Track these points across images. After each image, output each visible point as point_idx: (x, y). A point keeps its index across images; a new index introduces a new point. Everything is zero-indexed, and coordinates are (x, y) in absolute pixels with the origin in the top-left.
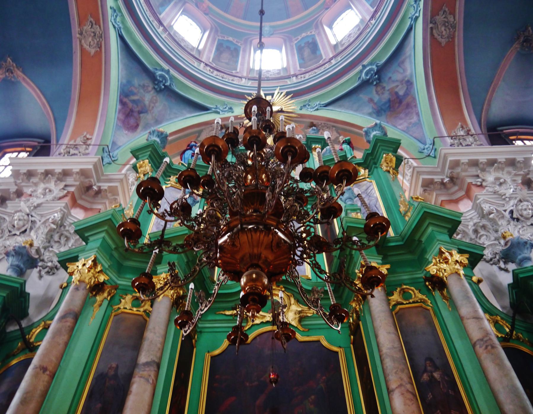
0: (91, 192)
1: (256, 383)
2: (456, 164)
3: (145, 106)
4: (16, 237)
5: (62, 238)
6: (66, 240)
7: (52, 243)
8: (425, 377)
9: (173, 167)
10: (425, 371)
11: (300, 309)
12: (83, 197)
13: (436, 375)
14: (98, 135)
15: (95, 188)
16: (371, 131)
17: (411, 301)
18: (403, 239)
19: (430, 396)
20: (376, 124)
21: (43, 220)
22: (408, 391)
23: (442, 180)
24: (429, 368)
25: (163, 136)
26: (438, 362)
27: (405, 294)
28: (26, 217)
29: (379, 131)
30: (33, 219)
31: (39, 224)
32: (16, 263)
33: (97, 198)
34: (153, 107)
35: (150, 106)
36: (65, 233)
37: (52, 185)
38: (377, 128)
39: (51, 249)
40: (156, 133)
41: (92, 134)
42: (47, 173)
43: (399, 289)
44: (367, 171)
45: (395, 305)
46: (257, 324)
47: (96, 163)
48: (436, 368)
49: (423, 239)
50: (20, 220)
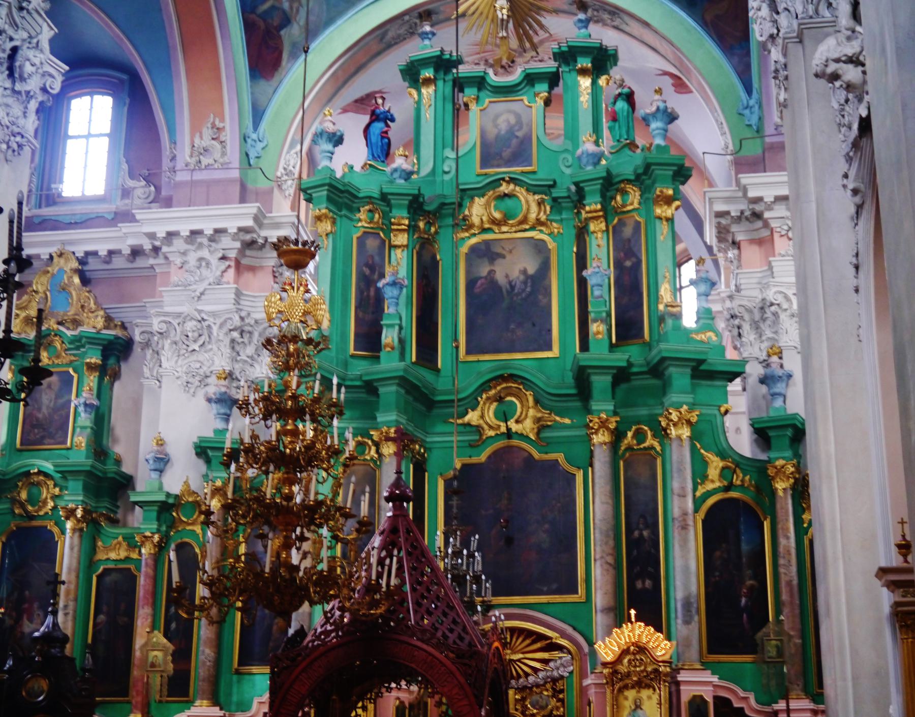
0: (255, 246)
1: (491, 511)
2: (759, 200)
3: (284, 12)
4: (195, 353)
5: (244, 335)
6: (250, 337)
7: (237, 348)
8: (636, 534)
9: (361, 195)
10: (638, 528)
11: (539, 415)
12: (248, 252)
13: (645, 533)
14: (232, 119)
15: (261, 241)
16: (651, 118)
17: (642, 446)
18: (648, 364)
19: (635, 552)
20: (658, 109)
21: (219, 322)
22: (607, 563)
23: (742, 212)
24: (641, 526)
25: (336, 138)
26: (650, 520)
27: (640, 436)
28: (199, 325)
29: (661, 120)
30: (207, 323)
31: (215, 329)
32: (222, 411)
33: (264, 250)
34: (298, 10)
35: (291, 8)
36: (247, 328)
37: (205, 253)
38: (659, 115)
39: (239, 358)
40: (325, 136)
41: (222, 120)
42: (195, 233)
43: (634, 428)
44: (637, 194)
45: (626, 449)
46: (491, 437)
47: (256, 215)
48: (647, 526)
49: (667, 373)
50: (193, 331)
